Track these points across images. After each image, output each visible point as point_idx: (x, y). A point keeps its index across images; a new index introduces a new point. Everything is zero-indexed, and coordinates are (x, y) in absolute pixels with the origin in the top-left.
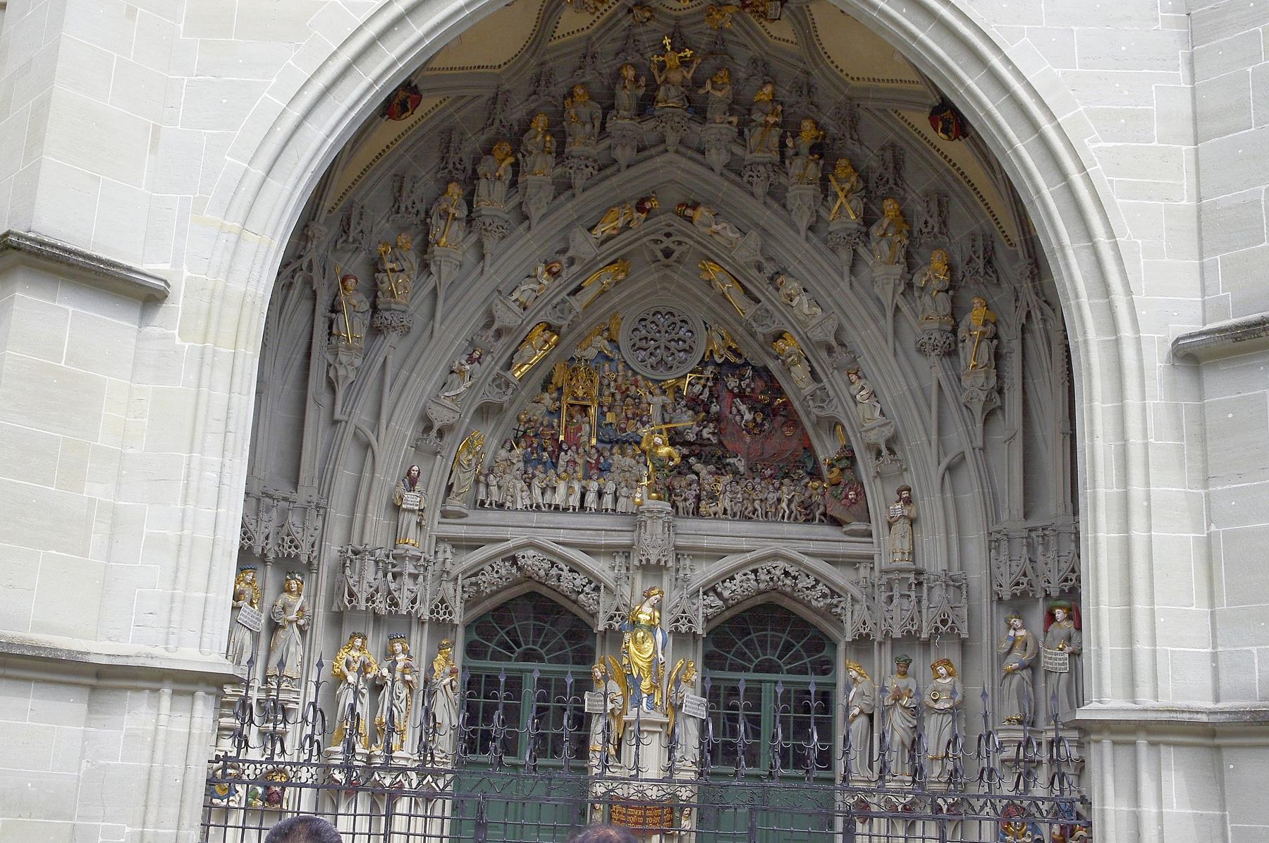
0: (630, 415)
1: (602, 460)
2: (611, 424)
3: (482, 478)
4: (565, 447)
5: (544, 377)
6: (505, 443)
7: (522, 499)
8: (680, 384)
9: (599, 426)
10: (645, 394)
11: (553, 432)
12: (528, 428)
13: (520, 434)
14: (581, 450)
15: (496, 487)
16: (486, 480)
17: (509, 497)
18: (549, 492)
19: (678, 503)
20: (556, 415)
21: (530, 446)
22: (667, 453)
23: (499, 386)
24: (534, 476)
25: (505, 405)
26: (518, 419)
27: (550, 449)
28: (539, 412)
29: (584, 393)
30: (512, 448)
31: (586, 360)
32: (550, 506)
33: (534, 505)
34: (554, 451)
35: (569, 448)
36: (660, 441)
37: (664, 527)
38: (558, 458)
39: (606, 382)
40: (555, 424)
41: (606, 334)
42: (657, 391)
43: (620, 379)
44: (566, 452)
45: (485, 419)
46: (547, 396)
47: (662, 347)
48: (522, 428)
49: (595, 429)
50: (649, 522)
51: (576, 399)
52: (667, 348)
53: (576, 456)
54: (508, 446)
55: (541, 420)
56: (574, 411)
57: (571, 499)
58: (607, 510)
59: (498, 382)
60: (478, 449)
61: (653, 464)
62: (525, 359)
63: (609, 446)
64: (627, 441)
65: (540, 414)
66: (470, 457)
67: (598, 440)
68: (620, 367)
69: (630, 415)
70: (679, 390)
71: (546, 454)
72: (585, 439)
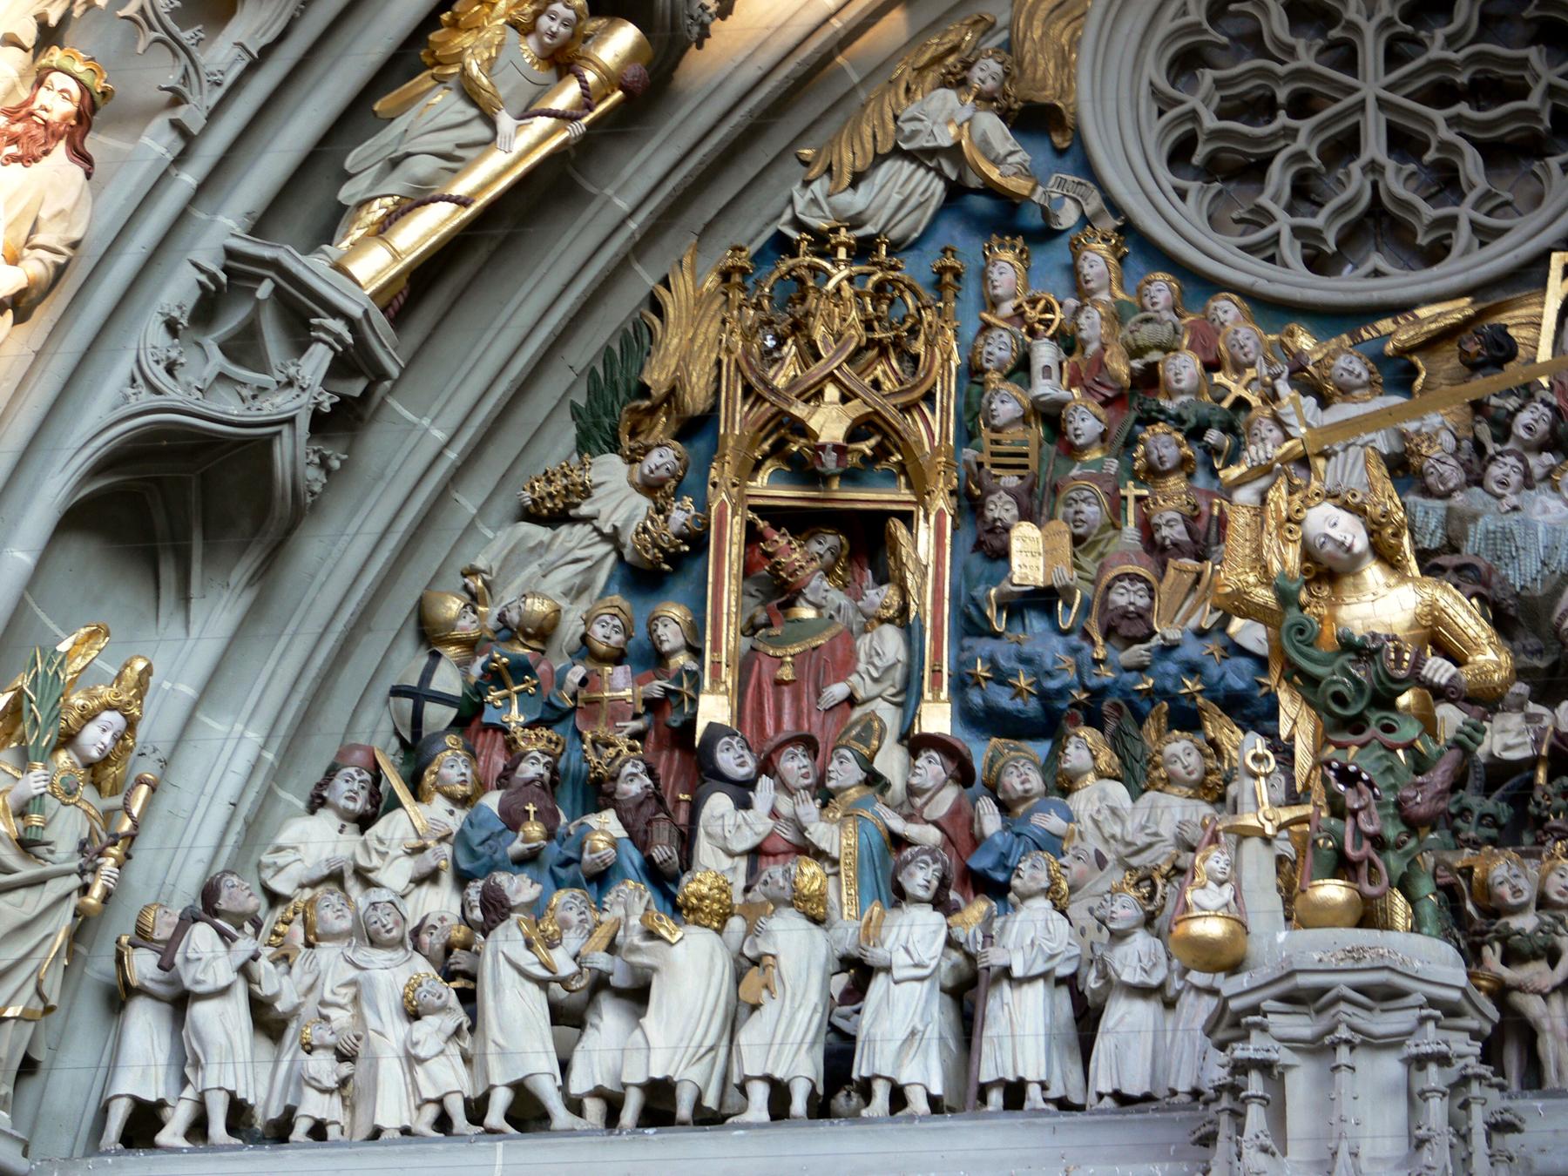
0: (1174, 532)
1: (990, 821)
2: (1044, 599)
3: (143, 965)
4: (732, 760)
5: (584, 351)
6: (331, 772)
7: (412, 1060)
8: (1513, 320)
9: (971, 624)
10: (1272, 397)
11: (656, 688)
12: (494, 677)
13: (438, 716)
14: (845, 772)
15: (236, 1010)
16: (166, 965)
17: (323, 1067)
18: (609, 1019)
19: (1533, 1006)
20: (682, 587)
21: (504, 780)
22: (1416, 623)
23: (243, 347)
24: (496, 908)
25: (283, 453)
26: (430, 634)
27: (633, 786)
28: (566, 575)
29: (854, 434)
30: (378, 805)
31: (863, 250)
32: (613, 1105)
33: (501, 1099)
34: (656, 797)
35: (767, 766)
36: (1350, 531)
37: (1415, 1099)
38: (686, 841)
39: (1000, 348)
40: (671, 636)
41: (986, 72)
42: (1350, 365)
43: (1092, 325)
44: (742, 793)
45: (168, 574)
46: (610, 471)
47: (1374, 145)
48: (448, 680)
49: (941, 653)
50: (1300, 1082)
51: (804, 470)
52: (1403, 142)
53: (809, 810)
54: (349, 790)
55: (571, 628)
56: (791, 552)
57: (751, 1035)
58: (1015, 1093)
59: (232, 321)
60: (96, 738)
61: (1307, 685)
62: (422, 166)
63: (1041, 749)
64: (1152, 695)
65: (576, 592)
66: (34, 782)
67: (967, 716)
68: (1097, 260)
69: (1174, 532)
70: (1501, 350)
71: (606, 827)
72: (888, 715)
